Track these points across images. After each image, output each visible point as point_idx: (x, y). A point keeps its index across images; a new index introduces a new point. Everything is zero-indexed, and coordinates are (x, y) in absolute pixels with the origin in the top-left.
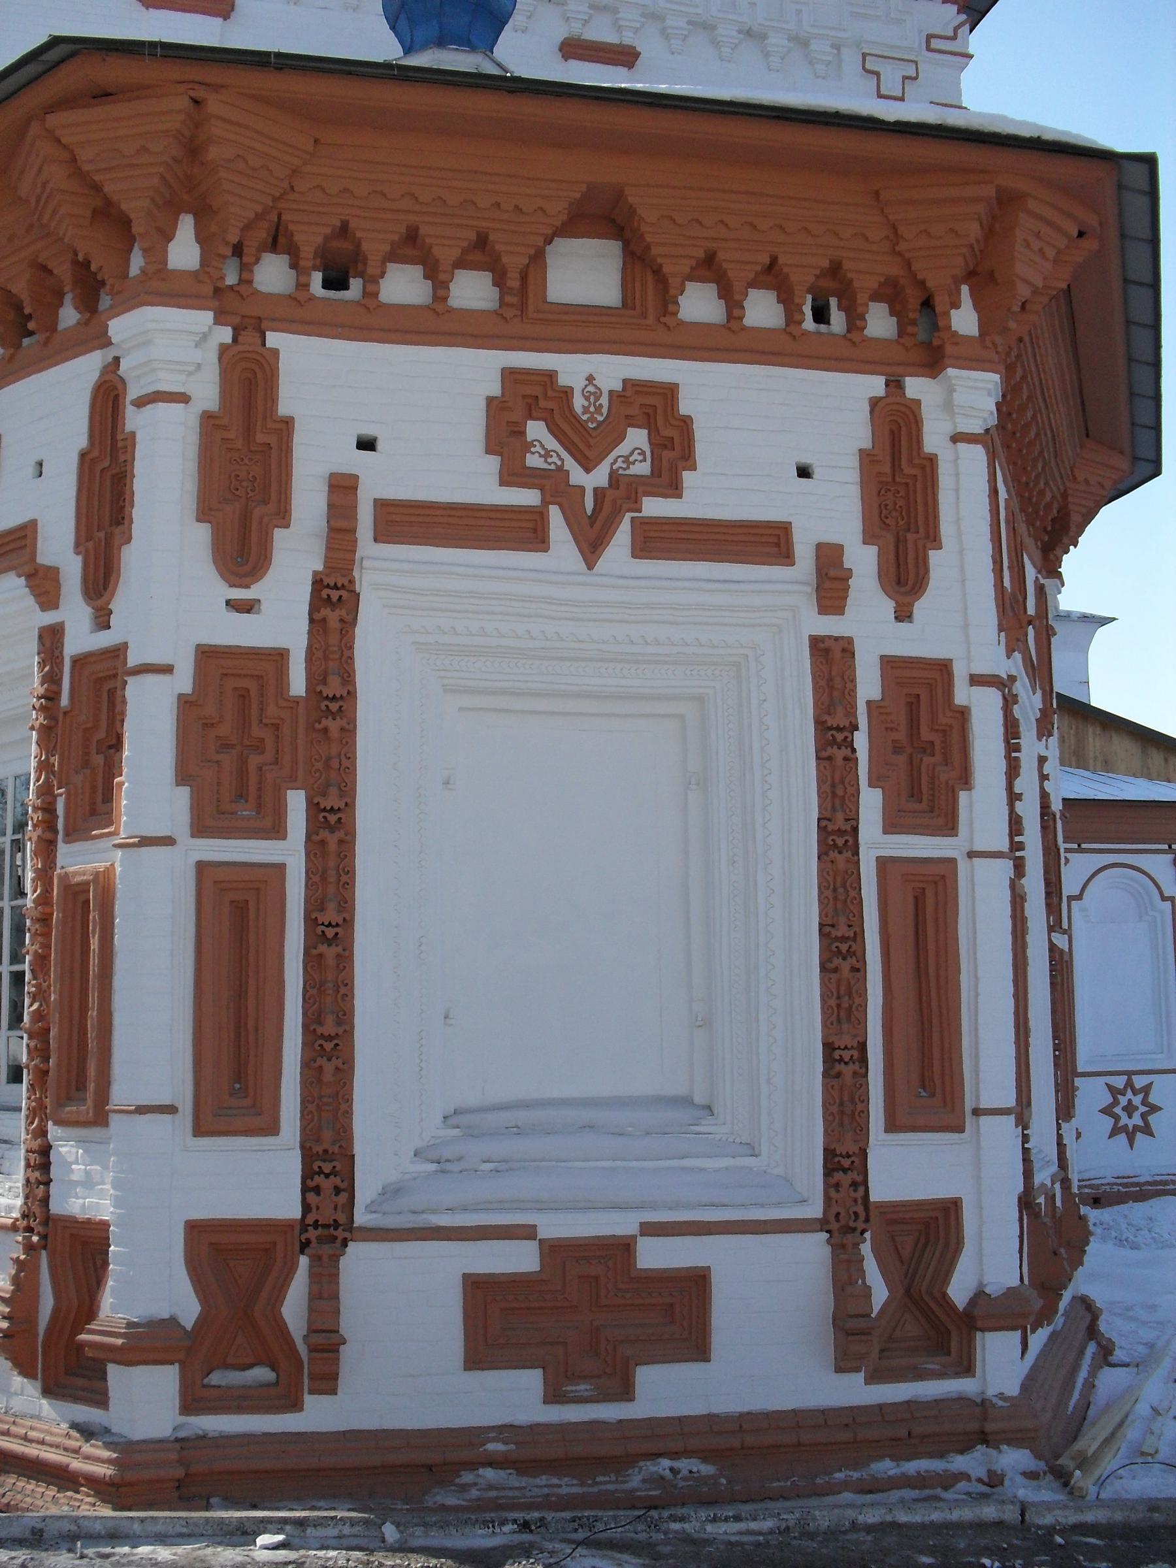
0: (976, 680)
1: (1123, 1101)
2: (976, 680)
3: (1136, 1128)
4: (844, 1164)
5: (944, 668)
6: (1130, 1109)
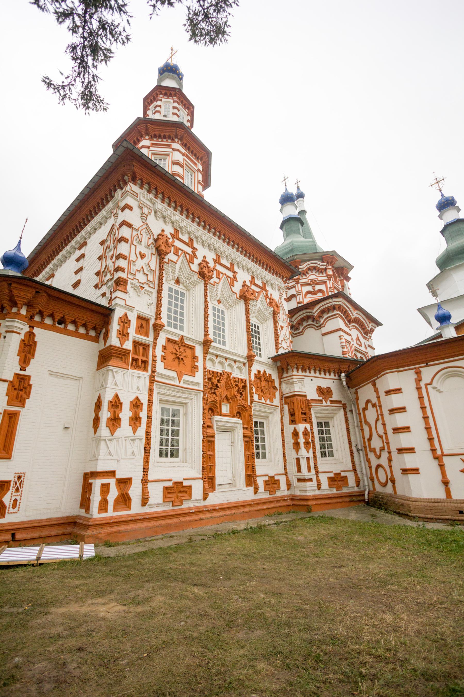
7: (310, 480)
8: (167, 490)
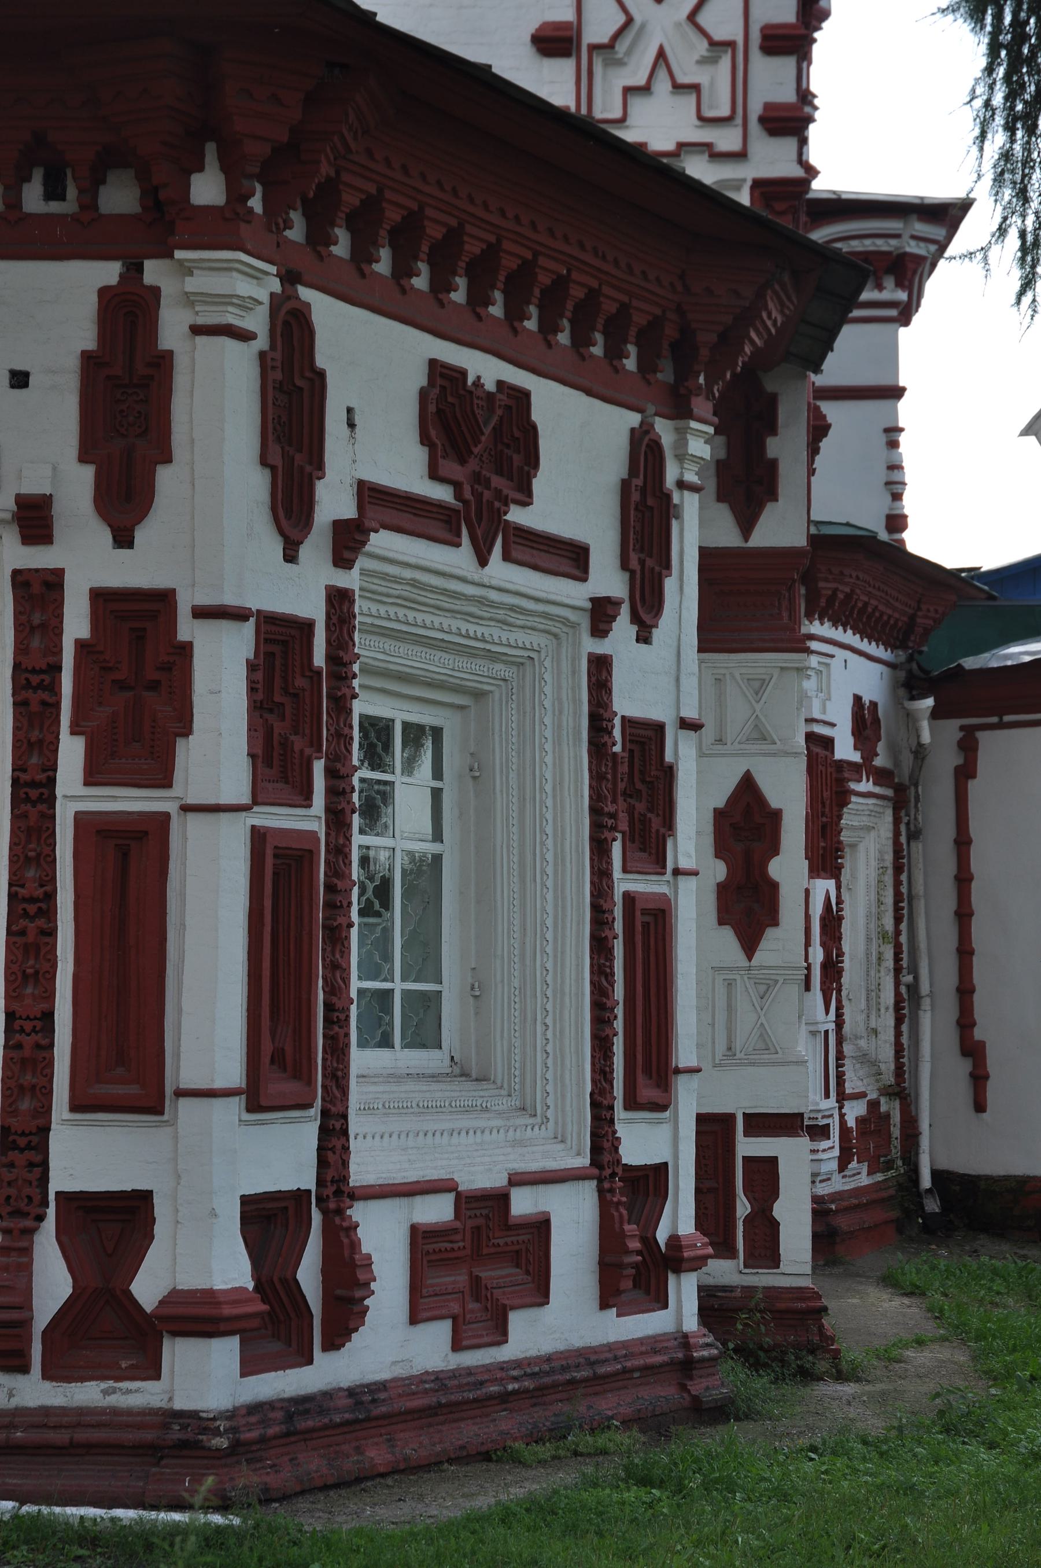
0: (201, 613)
2: (201, 613)
5: (165, 598)
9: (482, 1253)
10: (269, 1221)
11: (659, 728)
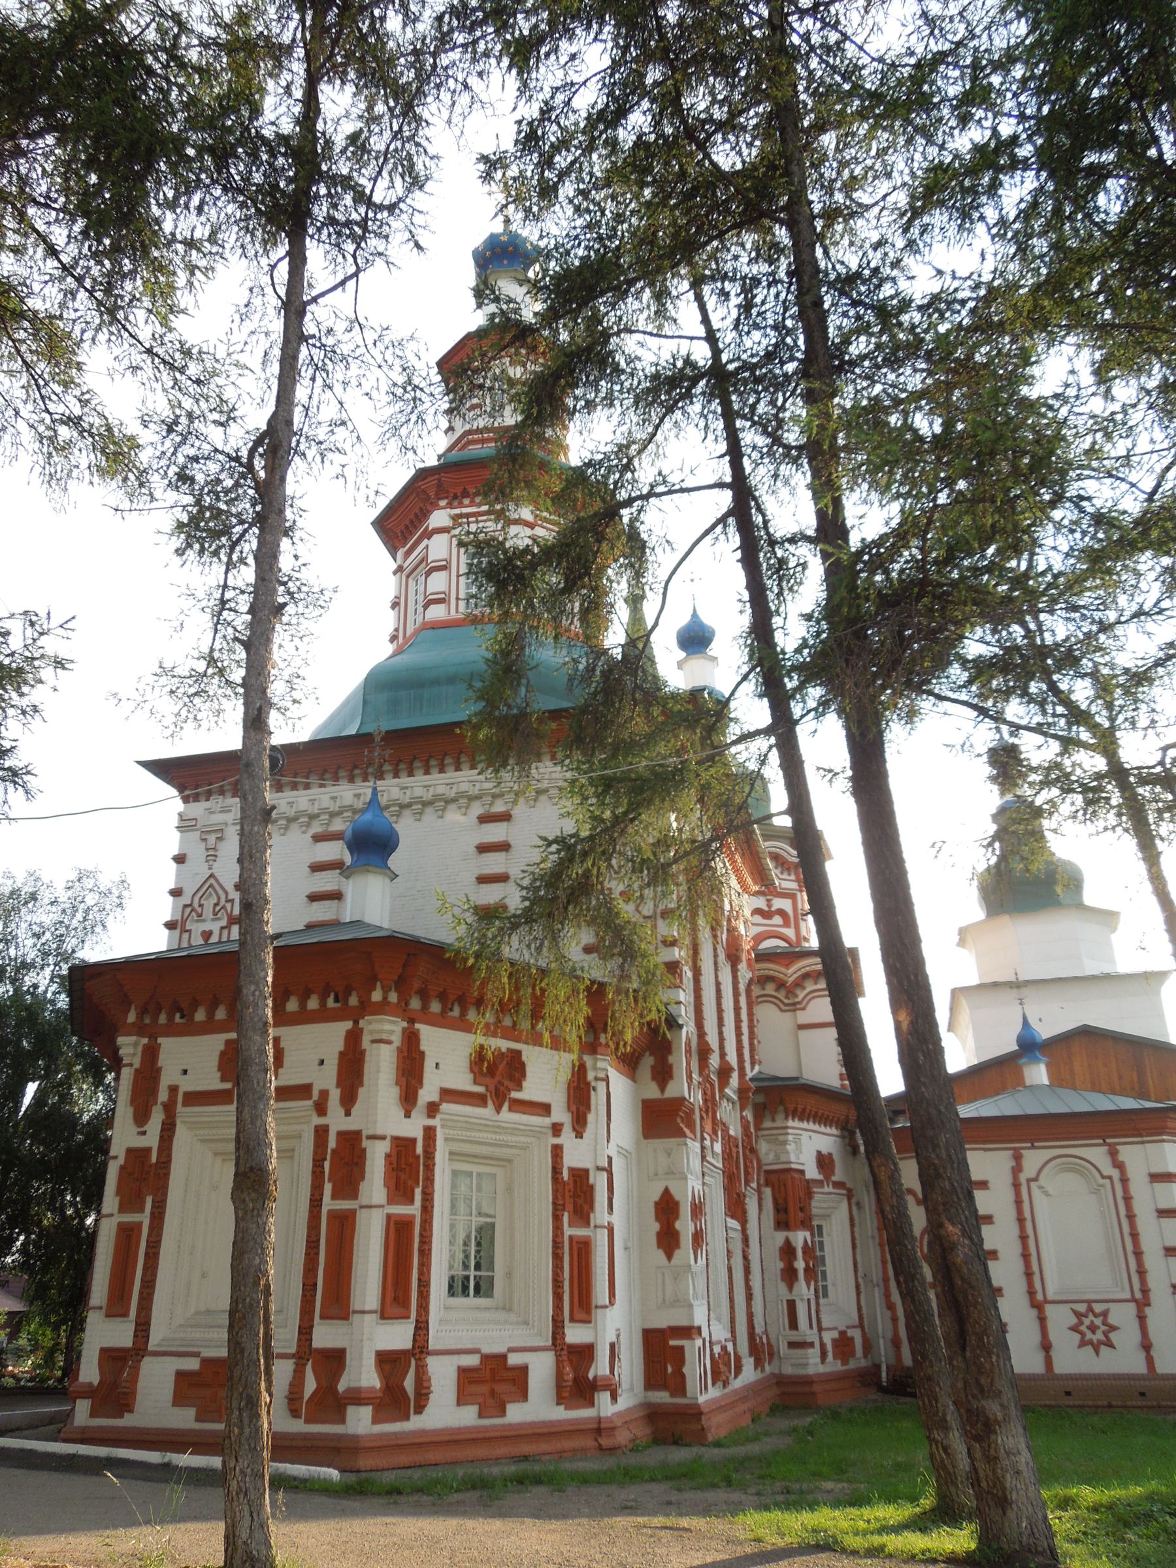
0: (370, 1137)
1: (1087, 1322)
2: (370, 1137)
3: (1100, 1342)
4: (305, 1331)
5: (358, 1133)
6: (1093, 1328)
7: (812, 1345)
8: (466, 1376)
9: (494, 1379)
10: (389, 1362)
11: (587, 1171)
